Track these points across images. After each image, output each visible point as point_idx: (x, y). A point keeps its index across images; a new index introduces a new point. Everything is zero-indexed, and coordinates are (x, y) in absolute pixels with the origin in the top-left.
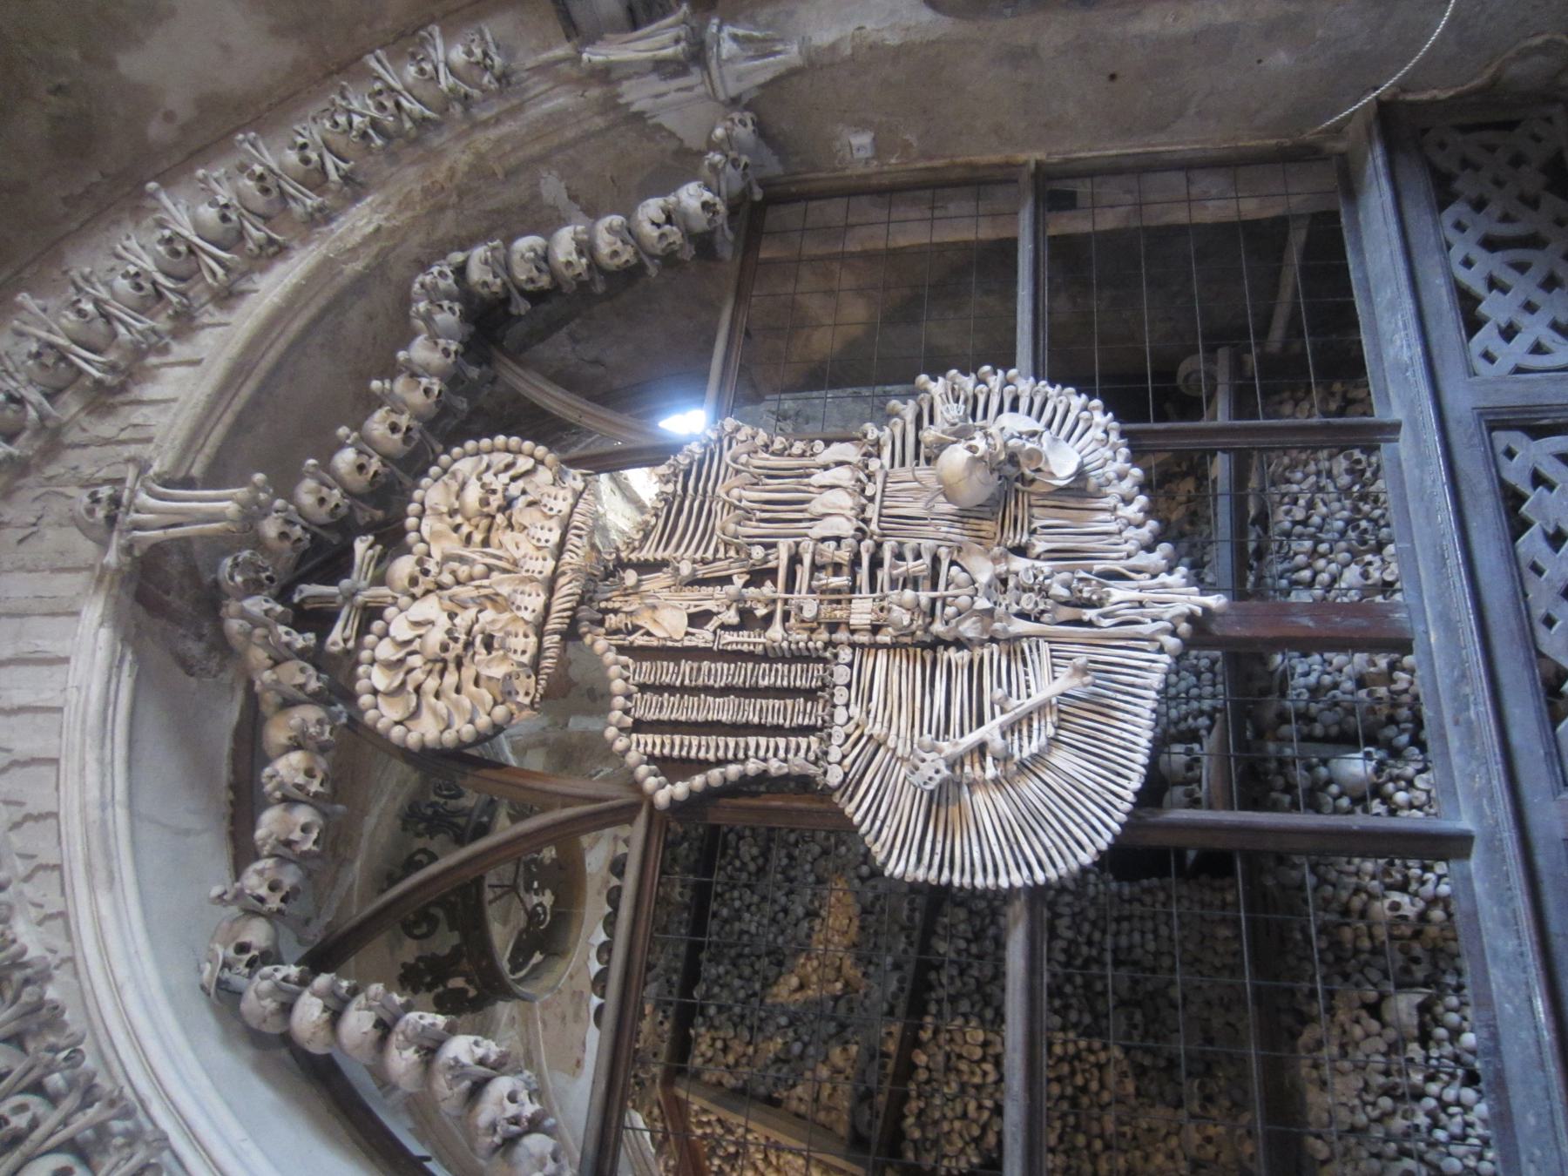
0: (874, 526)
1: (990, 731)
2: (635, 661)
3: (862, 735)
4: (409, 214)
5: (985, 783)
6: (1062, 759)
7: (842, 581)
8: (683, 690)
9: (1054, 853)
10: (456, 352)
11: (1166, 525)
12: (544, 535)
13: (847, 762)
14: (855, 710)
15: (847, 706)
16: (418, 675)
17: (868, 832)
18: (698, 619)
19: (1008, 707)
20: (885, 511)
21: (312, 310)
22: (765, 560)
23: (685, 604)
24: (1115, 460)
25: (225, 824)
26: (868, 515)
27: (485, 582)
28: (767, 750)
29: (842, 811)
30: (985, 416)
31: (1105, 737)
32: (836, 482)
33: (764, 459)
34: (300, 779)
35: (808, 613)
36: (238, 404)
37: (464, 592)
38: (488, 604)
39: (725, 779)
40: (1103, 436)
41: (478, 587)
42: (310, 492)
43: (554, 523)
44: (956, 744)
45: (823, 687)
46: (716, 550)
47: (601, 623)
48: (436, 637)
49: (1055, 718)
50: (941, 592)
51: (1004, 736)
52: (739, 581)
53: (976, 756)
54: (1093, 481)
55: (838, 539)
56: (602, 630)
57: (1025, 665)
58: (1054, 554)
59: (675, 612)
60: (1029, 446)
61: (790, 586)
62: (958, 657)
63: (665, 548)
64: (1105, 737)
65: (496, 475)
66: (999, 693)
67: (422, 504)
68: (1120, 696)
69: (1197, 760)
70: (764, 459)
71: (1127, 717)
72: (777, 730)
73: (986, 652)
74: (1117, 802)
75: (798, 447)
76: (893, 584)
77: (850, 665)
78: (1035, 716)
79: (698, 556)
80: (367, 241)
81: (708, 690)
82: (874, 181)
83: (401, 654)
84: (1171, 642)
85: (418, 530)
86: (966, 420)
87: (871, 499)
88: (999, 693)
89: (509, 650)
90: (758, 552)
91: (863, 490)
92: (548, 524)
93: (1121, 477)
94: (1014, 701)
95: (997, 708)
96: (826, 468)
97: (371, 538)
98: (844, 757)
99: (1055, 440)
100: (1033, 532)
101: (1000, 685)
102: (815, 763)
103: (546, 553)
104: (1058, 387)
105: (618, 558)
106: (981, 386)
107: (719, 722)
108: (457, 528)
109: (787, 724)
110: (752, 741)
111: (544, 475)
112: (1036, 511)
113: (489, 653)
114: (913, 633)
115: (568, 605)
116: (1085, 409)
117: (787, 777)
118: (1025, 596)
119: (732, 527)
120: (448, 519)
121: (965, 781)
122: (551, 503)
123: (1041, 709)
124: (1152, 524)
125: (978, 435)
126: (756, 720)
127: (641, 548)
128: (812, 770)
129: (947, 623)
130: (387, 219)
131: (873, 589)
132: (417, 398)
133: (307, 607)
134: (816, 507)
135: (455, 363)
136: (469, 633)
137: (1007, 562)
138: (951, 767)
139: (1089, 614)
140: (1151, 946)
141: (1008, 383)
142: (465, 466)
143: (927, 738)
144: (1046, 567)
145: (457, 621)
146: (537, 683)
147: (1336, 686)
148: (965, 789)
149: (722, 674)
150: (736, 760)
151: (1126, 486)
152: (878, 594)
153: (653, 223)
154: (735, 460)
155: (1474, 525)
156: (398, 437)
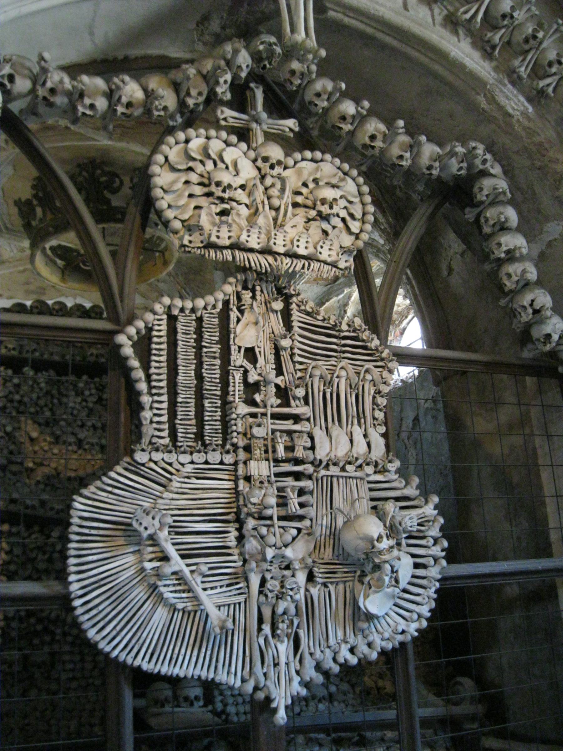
0: (323, 472)
1: (178, 563)
2: (218, 313)
3: (171, 474)
4: (523, 134)
5: (141, 562)
6: (161, 615)
7: (281, 452)
8: (199, 348)
10: (431, 174)
12: (302, 244)
13: (152, 465)
14: (189, 468)
15: (192, 462)
16: (200, 168)
17: (103, 483)
18: (251, 354)
19: (195, 575)
20: (335, 480)
21: (450, 78)
22: (295, 398)
23: (261, 345)
24: (382, 640)
25: (99, 56)
26: (332, 468)
27: (267, 207)
28: (158, 409)
29: (118, 464)
30: (409, 545)
31: (179, 644)
32: (355, 444)
33: (370, 391)
34: (124, 100)
35: (256, 431)
36: (380, 35)
37: (259, 195)
38: (252, 210)
39: (137, 381)
40: (400, 629)
41: (263, 202)
42: (324, 87)
43: (311, 250)
44: (166, 541)
45: (205, 445)
46: (301, 363)
47: (245, 288)
48: (226, 178)
49: (190, 608)
51: (174, 573)
52: (279, 380)
53: (160, 555)
54: (365, 625)
56: (239, 289)
57: (228, 585)
58: (309, 600)
59: (254, 339)
60: (387, 579)
61: (275, 416)
63: (300, 327)
64: (179, 644)
65: (345, 208)
66: (204, 569)
67: (322, 160)
68: (209, 653)
69: (192, 704)
70: (370, 391)
71: (194, 659)
72: (172, 414)
73: (235, 558)
74: (133, 654)
75: (380, 415)
76: (280, 489)
77: (222, 463)
78: (190, 595)
79: (296, 351)
80: (501, 108)
83: (213, 156)
84: (249, 687)
85: (303, 160)
86: (405, 532)
87: (343, 469)
88: (204, 569)
89: (219, 227)
90: (300, 392)
91: (350, 463)
92: (311, 246)
94: (199, 579)
96: (365, 436)
97: (297, 129)
98: (156, 463)
99: (393, 597)
100: (325, 585)
101: (210, 569)
102: (150, 443)
103: (289, 246)
104: (435, 596)
105: (292, 296)
106: (432, 541)
107: (177, 374)
108: (305, 185)
109: (177, 422)
110: (165, 398)
111: (348, 241)
112: (341, 586)
113: (217, 214)
114: (246, 506)
115: (253, 264)
116: (420, 616)
117: (139, 425)
118: (277, 583)
119: (317, 373)
120: (311, 179)
121: (141, 548)
122: (326, 247)
123: (196, 598)
124: (336, 669)
125: (392, 542)
126: (179, 400)
127: (300, 311)
128: (145, 440)
129: (255, 529)
130: (518, 121)
131: (276, 475)
132: (395, 151)
133: (248, 93)
134: (336, 431)
135: (424, 174)
136: (231, 199)
137: (302, 569)
138: (151, 537)
139: (267, 629)
141: (436, 560)
142: (350, 186)
143: (170, 520)
144: (300, 596)
145: (240, 191)
146: (198, 248)
148: (136, 548)
149: (211, 373)
150: (150, 387)
151: (363, 649)
152: (273, 478)
153: (533, 301)
154: (367, 371)
156: (367, 141)
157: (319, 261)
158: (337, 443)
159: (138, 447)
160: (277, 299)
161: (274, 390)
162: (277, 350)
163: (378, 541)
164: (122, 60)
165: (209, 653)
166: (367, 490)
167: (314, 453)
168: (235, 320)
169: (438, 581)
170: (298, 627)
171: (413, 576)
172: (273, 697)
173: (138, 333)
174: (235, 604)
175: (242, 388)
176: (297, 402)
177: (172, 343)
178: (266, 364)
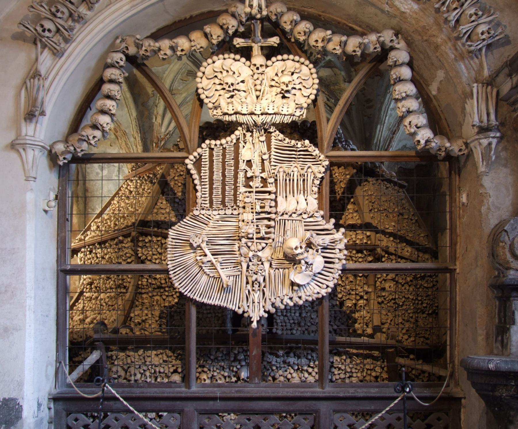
1: (210, 257)
8: (224, 162)
9: (178, 276)
11: (282, 311)
12: (271, 108)
14: (218, 217)
15: (219, 214)
18: (249, 163)
20: (286, 221)
26: (285, 215)
30: (322, 252)
35: (247, 200)
40: (316, 291)
43: (276, 110)
45: (225, 206)
47: (248, 131)
48: (230, 80)
49: (216, 276)
50: (255, 240)
52: (263, 175)
53: (204, 254)
55: (276, 206)
56: (244, 132)
62: (236, 248)
68: (224, 295)
71: (218, 298)
72: (211, 193)
75: (316, 189)
76: (257, 226)
77: (232, 214)
79: (272, 160)
81: (224, 170)
82: (453, 205)
85: (277, 61)
87: (291, 216)
88: (220, 260)
90: (272, 180)
91: (295, 213)
93: (300, 298)
94: (219, 264)
95: (216, 260)
96: (306, 200)
98: (203, 215)
105: (272, 132)
106: (338, 251)
109: (213, 196)
110: (208, 186)
119: (281, 170)
122: (285, 107)
126: (214, 187)
127: (276, 140)
131: (257, 219)
134: (290, 197)
138: (199, 246)
139: (249, 287)
140: (205, 312)
143: (206, 239)
145: (241, 84)
147: (273, 370)
149: (230, 173)
152: (255, 221)
155: (278, 403)
157: (281, 114)
158: (290, 203)
159: (195, 208)
160: (262, 135)
161: (260, 179)
162: (263, 160)
163: (295, 249)
164: (189, 18)
165: (224, 295)
166: (303, 226)
167: (276, 209)
168: (242, 147)
169: (341, 270)
170: (265, 287)
171: (324, 267)
172: (251, 316)
173: (195, 157)
174: (236, 276)
175: (244, 180)
176: (271, 185)
177: (211, 161)
178: (256, 168)
